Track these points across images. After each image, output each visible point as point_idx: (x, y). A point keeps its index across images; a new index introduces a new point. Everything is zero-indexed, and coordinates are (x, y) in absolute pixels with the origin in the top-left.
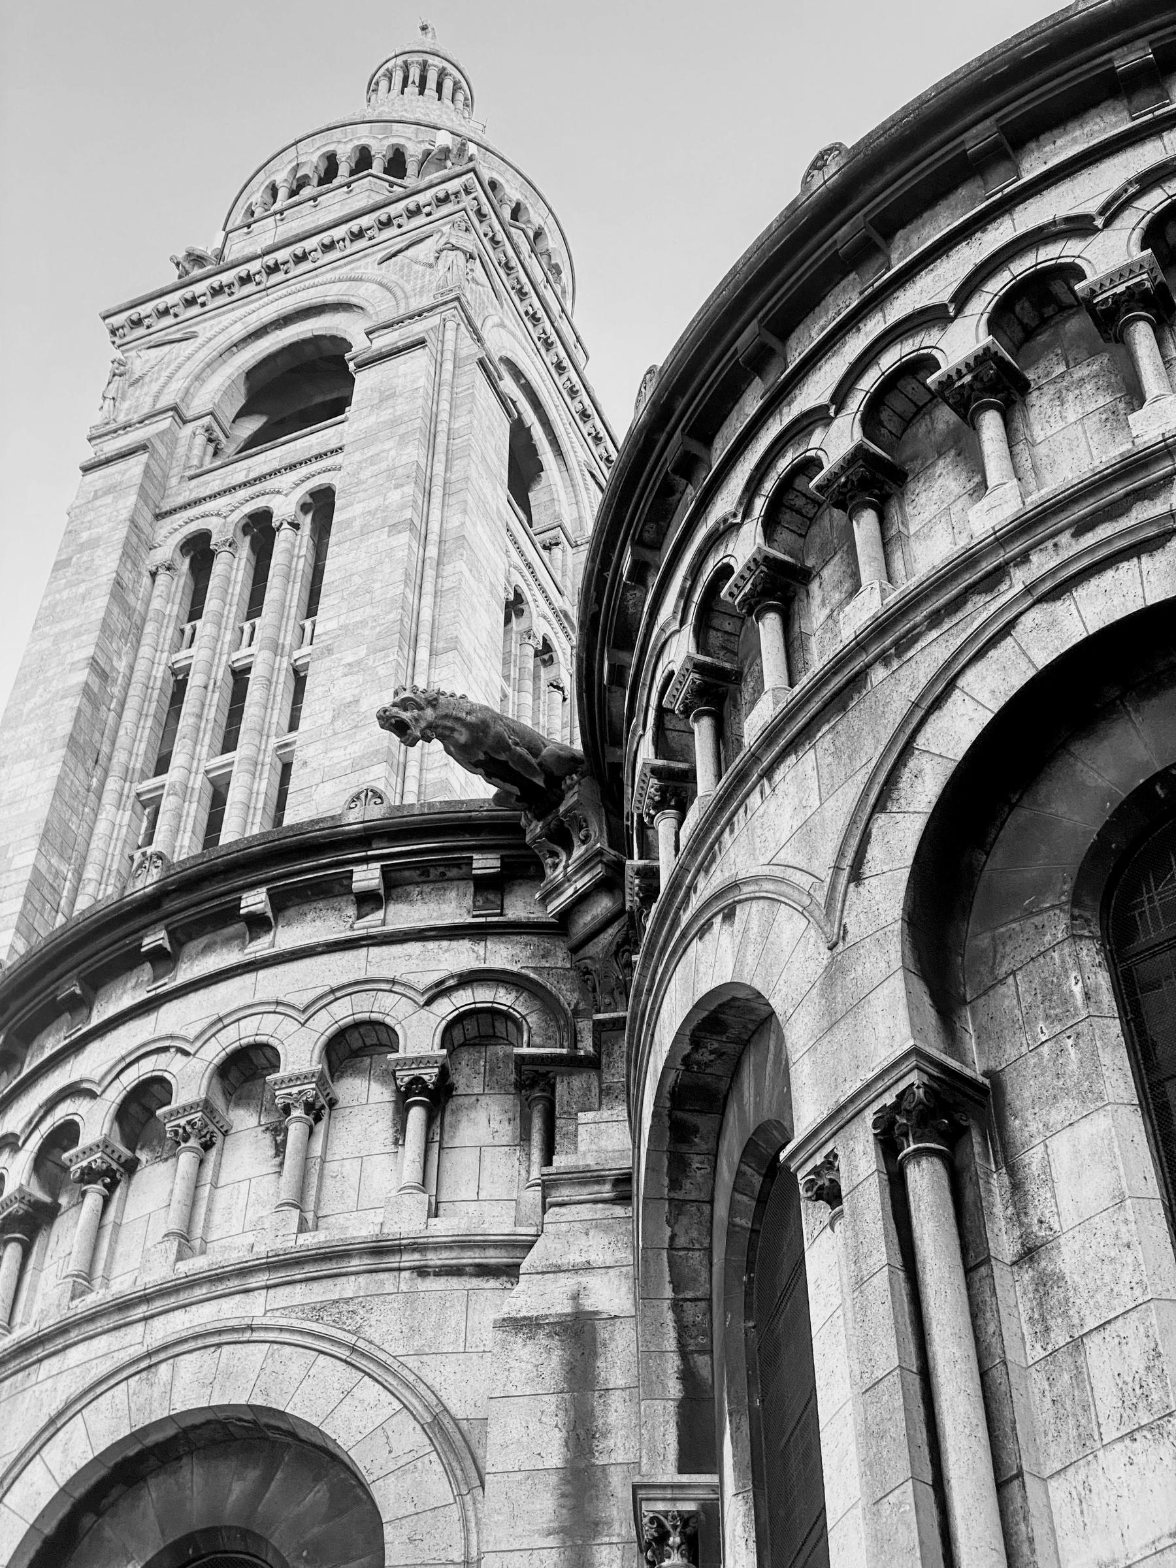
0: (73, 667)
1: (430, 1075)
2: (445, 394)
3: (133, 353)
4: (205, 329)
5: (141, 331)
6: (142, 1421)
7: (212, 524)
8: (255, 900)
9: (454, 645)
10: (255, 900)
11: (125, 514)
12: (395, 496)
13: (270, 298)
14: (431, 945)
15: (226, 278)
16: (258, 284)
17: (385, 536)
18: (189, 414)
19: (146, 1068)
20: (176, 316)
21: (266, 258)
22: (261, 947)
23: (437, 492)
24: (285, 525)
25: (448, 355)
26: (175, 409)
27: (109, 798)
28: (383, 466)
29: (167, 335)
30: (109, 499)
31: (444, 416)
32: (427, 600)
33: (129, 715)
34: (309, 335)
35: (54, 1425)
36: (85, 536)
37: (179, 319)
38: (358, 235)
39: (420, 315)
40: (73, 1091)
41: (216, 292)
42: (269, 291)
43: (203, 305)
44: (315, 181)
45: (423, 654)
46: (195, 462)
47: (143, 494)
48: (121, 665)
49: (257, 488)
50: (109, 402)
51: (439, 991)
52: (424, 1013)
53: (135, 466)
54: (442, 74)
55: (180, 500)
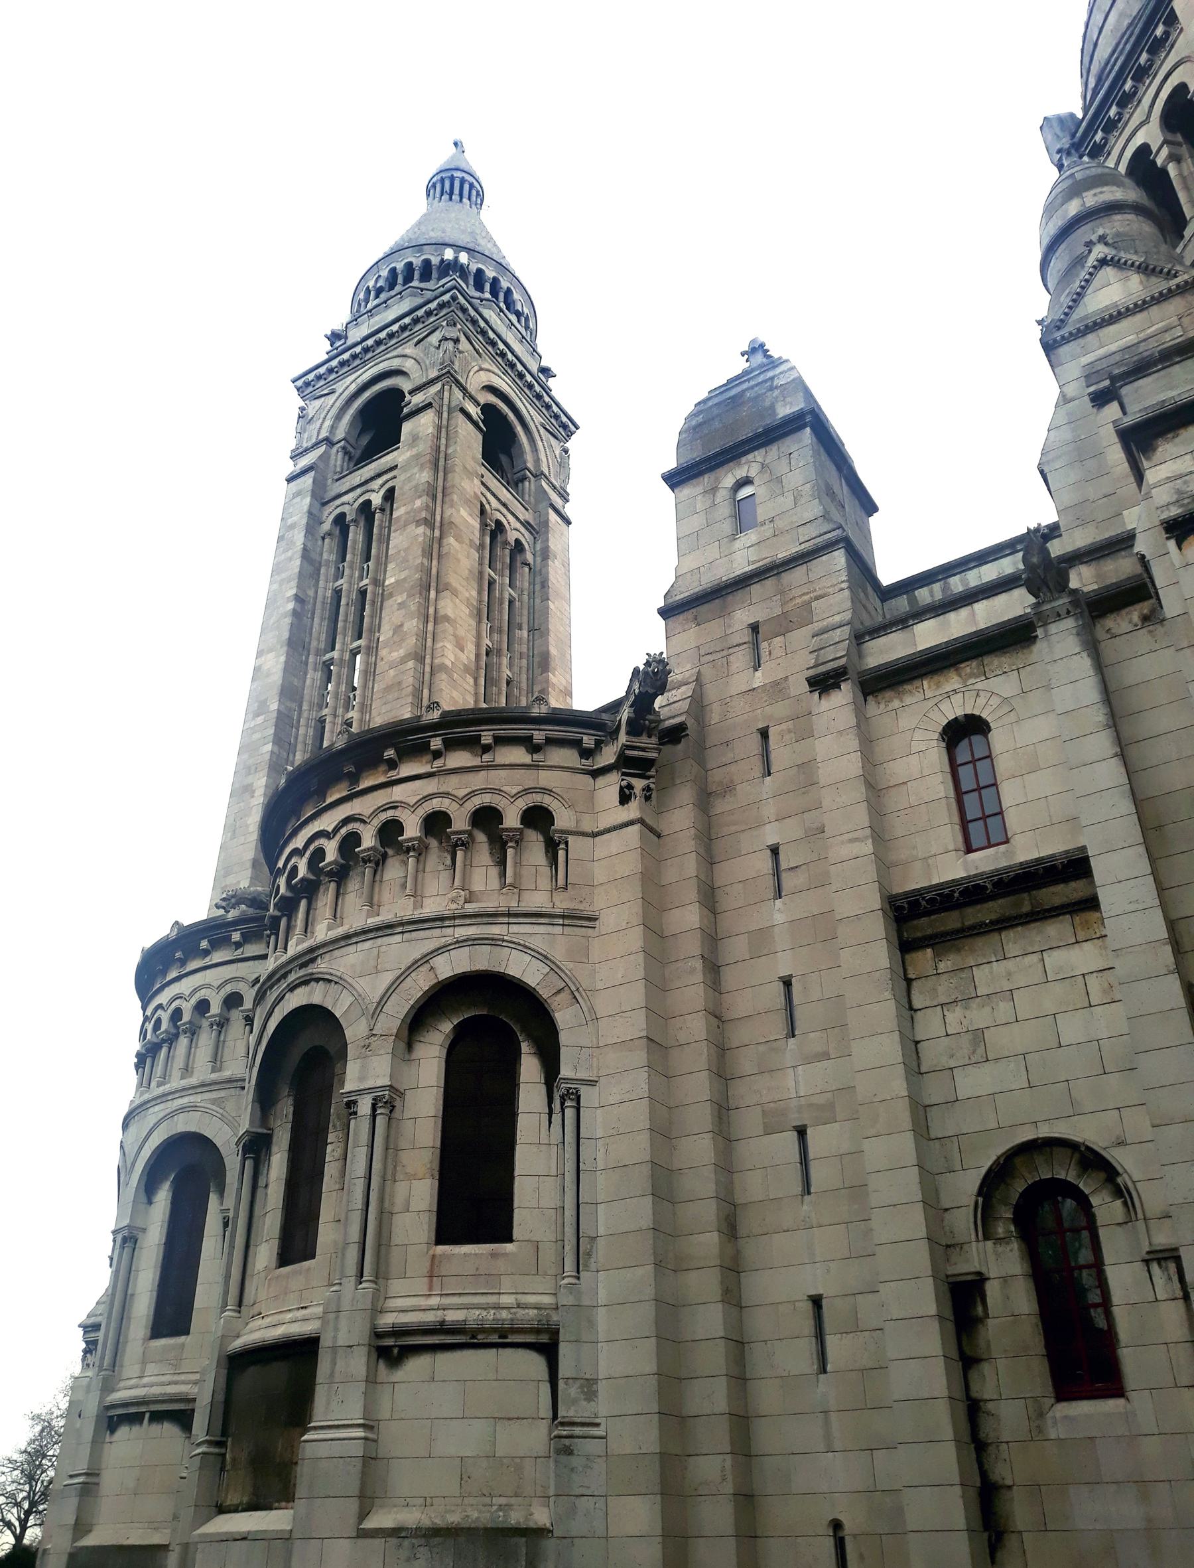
2: (443, 434)
3: (307, 402)
4: (339, 387)
5: (311, 389)
6: (171, 1134)
7: (346, 509)
9: (447, 587)
11: (306, 508)
13: (368, 366)
14: (256, 962)
16: (361, 359)
20: (325, 379)
22: (207, 961)
23: (439, 495)
25: (445, 408)
26: (327, 439)
27: (310, 666)
29: (322, 391)
30: (298, 499)
31: (443, 448)
32: (435, 563)
33: (316, 620)
40: (160, 1006)
43: (337, 372)
44: (387, 289)
45: (433, 594)
46: (338, 469)
47: (314, 495)
48: (311, 593)
52: (251, 990)
53: (308, 480)
54: (463, 181)
55: (332, 494)
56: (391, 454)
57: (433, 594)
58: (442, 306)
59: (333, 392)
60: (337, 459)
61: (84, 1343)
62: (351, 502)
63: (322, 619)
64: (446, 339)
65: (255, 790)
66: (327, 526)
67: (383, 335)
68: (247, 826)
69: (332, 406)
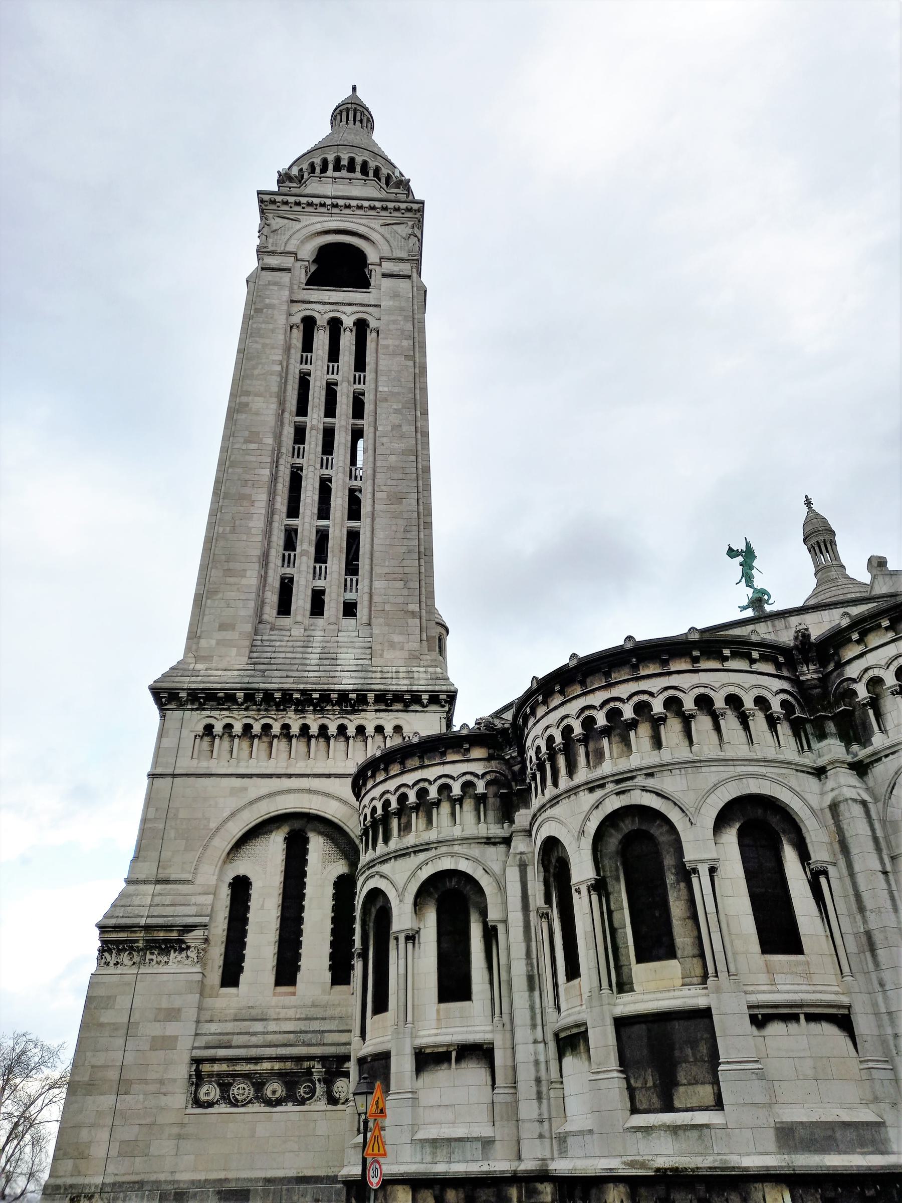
0: (274, 362)
1: (781, 716)
4: (306, 220)
8: (726, 652)
10: (726, 652)
12: (405, 343)
13: (334, 218)
14: (771, 678)
15: (316, 201)
16: (328, 210)
17: (403, 359)
18: (299, 257)
19: (702, 690)
20: (291, 207)
21: (333, 200)
24: (348, 329)
28: (399, 327)
29: (285, 214)
30: (276, 288)
32: (418, 391)
34: (348, 242)
35: (715, 787)
36: (267, 301)
38: (373, 208)
41: (310, 204)
45: (418, 414)
50: (264, 237)
51: (777, 693)
53: (285, 277)
57: (418, 414)
58: (409, 210)
61: (100, 942)
62: (322, 312)
63: (293, 389)
64: (416, 236)
65: (253, 502)
66: (297, 319)
67: (354, 203)
68: (251, 528)
69: (298, 231)
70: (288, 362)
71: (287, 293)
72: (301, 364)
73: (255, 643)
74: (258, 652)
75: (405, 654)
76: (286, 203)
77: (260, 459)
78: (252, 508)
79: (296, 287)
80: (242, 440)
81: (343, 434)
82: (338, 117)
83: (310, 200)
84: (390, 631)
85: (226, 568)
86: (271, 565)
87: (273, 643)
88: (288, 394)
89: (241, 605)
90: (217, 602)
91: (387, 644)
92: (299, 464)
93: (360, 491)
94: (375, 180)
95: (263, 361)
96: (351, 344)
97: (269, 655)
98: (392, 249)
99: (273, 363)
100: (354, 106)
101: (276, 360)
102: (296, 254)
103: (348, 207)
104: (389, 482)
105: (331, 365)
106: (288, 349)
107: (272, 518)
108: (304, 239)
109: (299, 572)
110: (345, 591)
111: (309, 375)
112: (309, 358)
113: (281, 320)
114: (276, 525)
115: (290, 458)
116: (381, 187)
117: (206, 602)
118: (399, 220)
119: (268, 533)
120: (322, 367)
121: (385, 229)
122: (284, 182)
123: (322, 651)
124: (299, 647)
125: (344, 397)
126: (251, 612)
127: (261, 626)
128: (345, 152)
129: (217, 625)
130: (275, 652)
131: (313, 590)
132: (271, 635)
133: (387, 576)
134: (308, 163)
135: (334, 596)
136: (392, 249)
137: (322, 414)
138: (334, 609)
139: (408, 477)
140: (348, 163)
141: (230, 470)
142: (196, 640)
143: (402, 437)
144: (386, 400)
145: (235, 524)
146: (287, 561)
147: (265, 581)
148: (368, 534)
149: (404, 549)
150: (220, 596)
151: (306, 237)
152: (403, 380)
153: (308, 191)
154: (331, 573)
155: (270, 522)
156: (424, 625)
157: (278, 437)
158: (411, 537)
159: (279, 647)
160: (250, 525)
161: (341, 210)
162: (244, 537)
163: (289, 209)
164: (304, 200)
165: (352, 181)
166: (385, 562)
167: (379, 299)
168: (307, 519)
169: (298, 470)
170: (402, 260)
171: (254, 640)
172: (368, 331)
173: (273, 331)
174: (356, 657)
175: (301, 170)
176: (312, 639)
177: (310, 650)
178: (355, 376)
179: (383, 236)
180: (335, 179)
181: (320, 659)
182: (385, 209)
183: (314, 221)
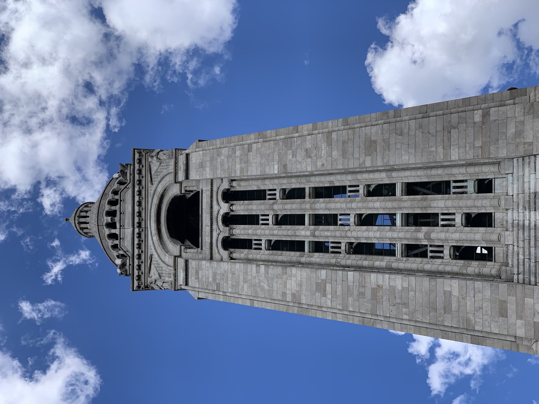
0: (258, 272)
4: (151, 250)
7: (221, 237)
12: (238, 153)
13: (149, 226)
16: (142, 231)
17: (251, 153)
18: (178, 254)
20: (142, 262)
21: (135, 227)
24: (231, 208)
28: (226, 160)
29: (147, 267)
30: (200, 272)
37: (144, 262)
39: (176, 163)
41: (139, 247)
42: (146, 227)
43: (142, 252)
49: (214, 221)
53: (192, 264)
56: (203, 199)
59: (152, 255)
60: (191, 253)
62: (218, 231)
64: (158, 153)
65: (378, 286)
66: (225, 254)
67: (137, 209)
69: (159, 256)
70: (259, 261)
71: (204, 262)
72: (261, 249)
73: (521, 281)
74: (530, 276)
75: (528, 118)
76: (139, 266)
77: (339, 281)
78: (384, 287)
79: (200, 256)
80: (324, 298)
81: (318, 206)
82: (85, 231)
83: (136, 246)
84: (504, 137)
85: (443, 311)
86: (441, 268)
87: (521, 261)
88: (285, 259)
89: (480, 295)
90: (477, 320)
91: (518, 140)
92: (346, 246)
93: (369, 186)
94: (120, 193)
95: (257, 281)
96: (243, 204)
97: (532, 264)
98: (169, 174)
99: (259, 273)
100: (77, 218)
101: (256, 270)
102: (175, 257)
103: (140, 213)
104: (356, 156)
105: (261, 222)
106: (249, 261)
107: (395, 270)
108: (165, 250)
109: (447, 240)
110: (466, 193)
111: (270, 241)
112: (256, 242)
113: (226, 266)
114: (401, 265)
115: (341, 255)
116: (126, 187)
117: (479, 331)
118: (148, 169)
119: (410, 272)
120: (263, 229)
121: (155, 181)
122: (126, 271)
123: (527, 210)
124: (523, 234)
125: (286, 207)
126: (487, 285)
127: (503, 277)
128: (103, 219)
129: (500, 318)
130: (530, 259)
131: (466, 226)
132: (513, 265)
133: (447, 147)
134: (112, 251)
135: (470, 203)
136: (169, 174)
137: (302, 227)
138: (484, 202)
139: (351, 137)
140: (110, 216)
141: (351, 309)
142: (518, 342)
143: (316, 147)
144: (285, 166)
145: (399, 304)
146: (438, 252)
147: (457, 274)
148: (408, 173)
149: (419, 133)
150: (472, 318)
151: (164, 248)
152: (268, 152)
153: (130, 249)
154: (447, 208)
155: (398, 271)
156: (497, 104)
157: (321, 266)
158: (407, 128)
159: (524, 255)
160: (400, 288)
161: (143, 220)
162: (412, 294)
163: (144, 264)
164: (136, 251)
165: (122, 212)
166: (432, 152)
167: (207, 179)
168: (395, 235)
169: (352, 248)
170: (176, 163)
171: (518, 282)
172: (232, 189)
173: (233, 274)
174: (533, 172)
175: (118, 257)
176: (516, 222)
177: (527, 223)
178: (270, 199)
179: (160, 182)
180: (121, 226)
181: (535, 210)
182: (140, 182)
183: (151, 242)
